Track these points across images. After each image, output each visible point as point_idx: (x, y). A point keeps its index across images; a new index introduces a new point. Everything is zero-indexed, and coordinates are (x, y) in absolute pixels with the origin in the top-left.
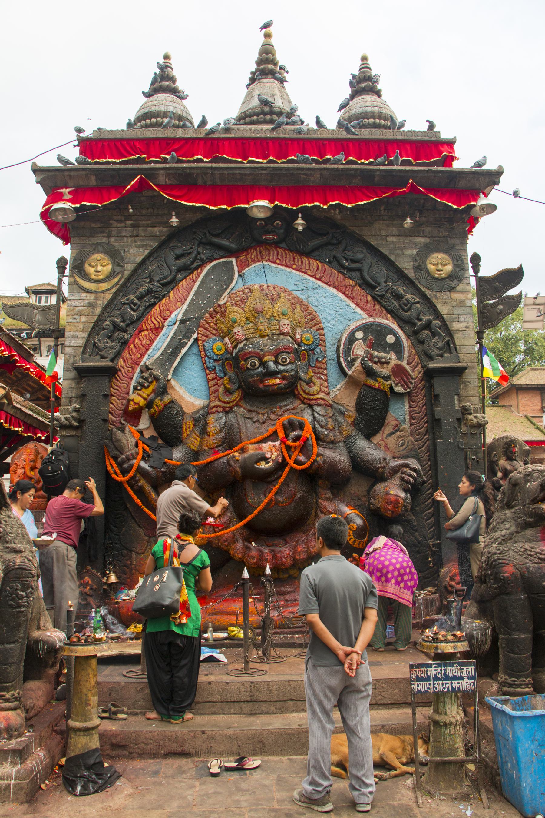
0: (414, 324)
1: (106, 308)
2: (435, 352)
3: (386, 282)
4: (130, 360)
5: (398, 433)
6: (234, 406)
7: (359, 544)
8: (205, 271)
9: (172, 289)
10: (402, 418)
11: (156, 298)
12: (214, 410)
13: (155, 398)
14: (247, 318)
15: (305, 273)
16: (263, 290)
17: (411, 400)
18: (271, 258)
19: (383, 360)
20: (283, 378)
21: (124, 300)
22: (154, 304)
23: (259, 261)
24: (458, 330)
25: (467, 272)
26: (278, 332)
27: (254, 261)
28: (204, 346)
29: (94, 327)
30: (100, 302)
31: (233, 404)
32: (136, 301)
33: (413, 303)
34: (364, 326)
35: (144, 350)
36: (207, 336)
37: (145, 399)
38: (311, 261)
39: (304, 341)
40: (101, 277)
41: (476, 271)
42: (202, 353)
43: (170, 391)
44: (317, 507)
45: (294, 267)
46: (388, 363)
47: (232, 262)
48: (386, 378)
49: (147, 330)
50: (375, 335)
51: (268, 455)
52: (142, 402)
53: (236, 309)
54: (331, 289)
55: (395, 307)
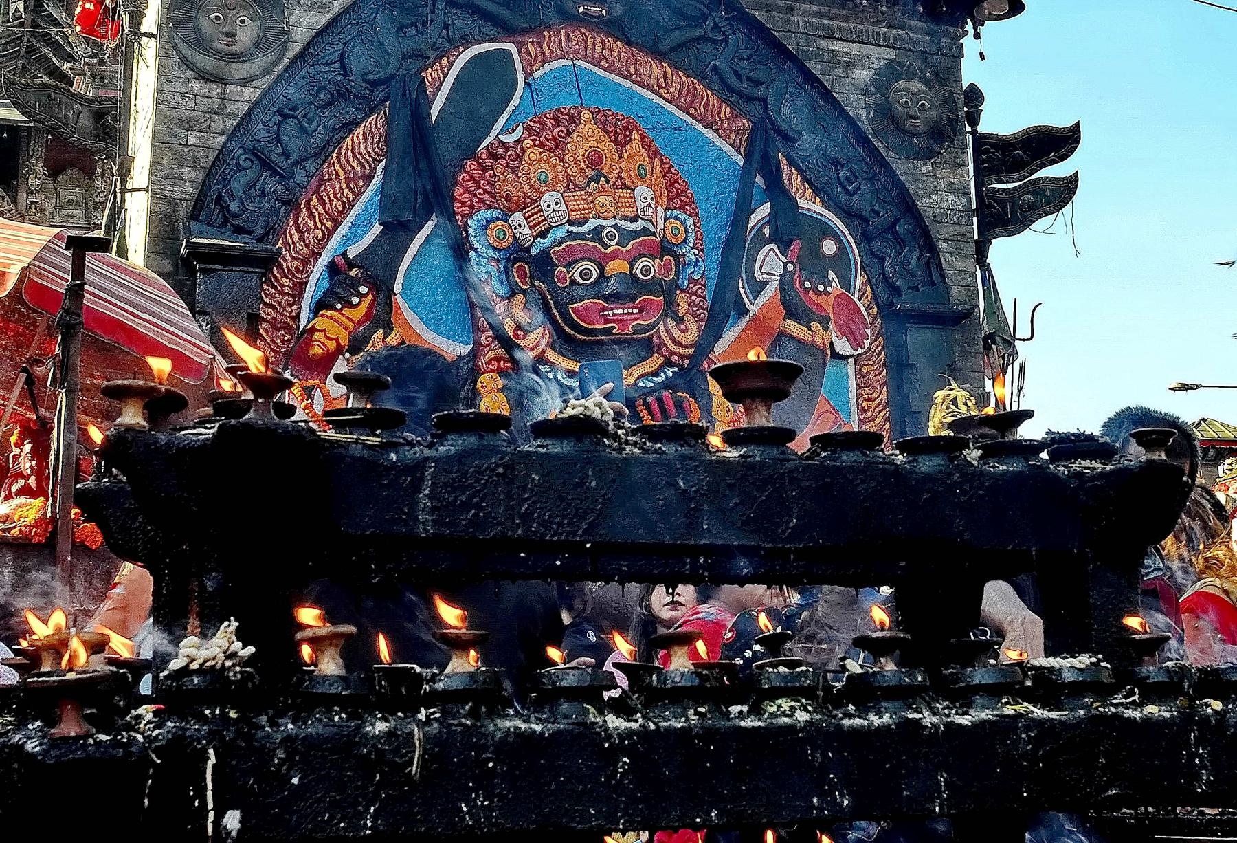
19: (821, 288)
26: (629, 212)
36: (472, 207)
54: (709, 133)
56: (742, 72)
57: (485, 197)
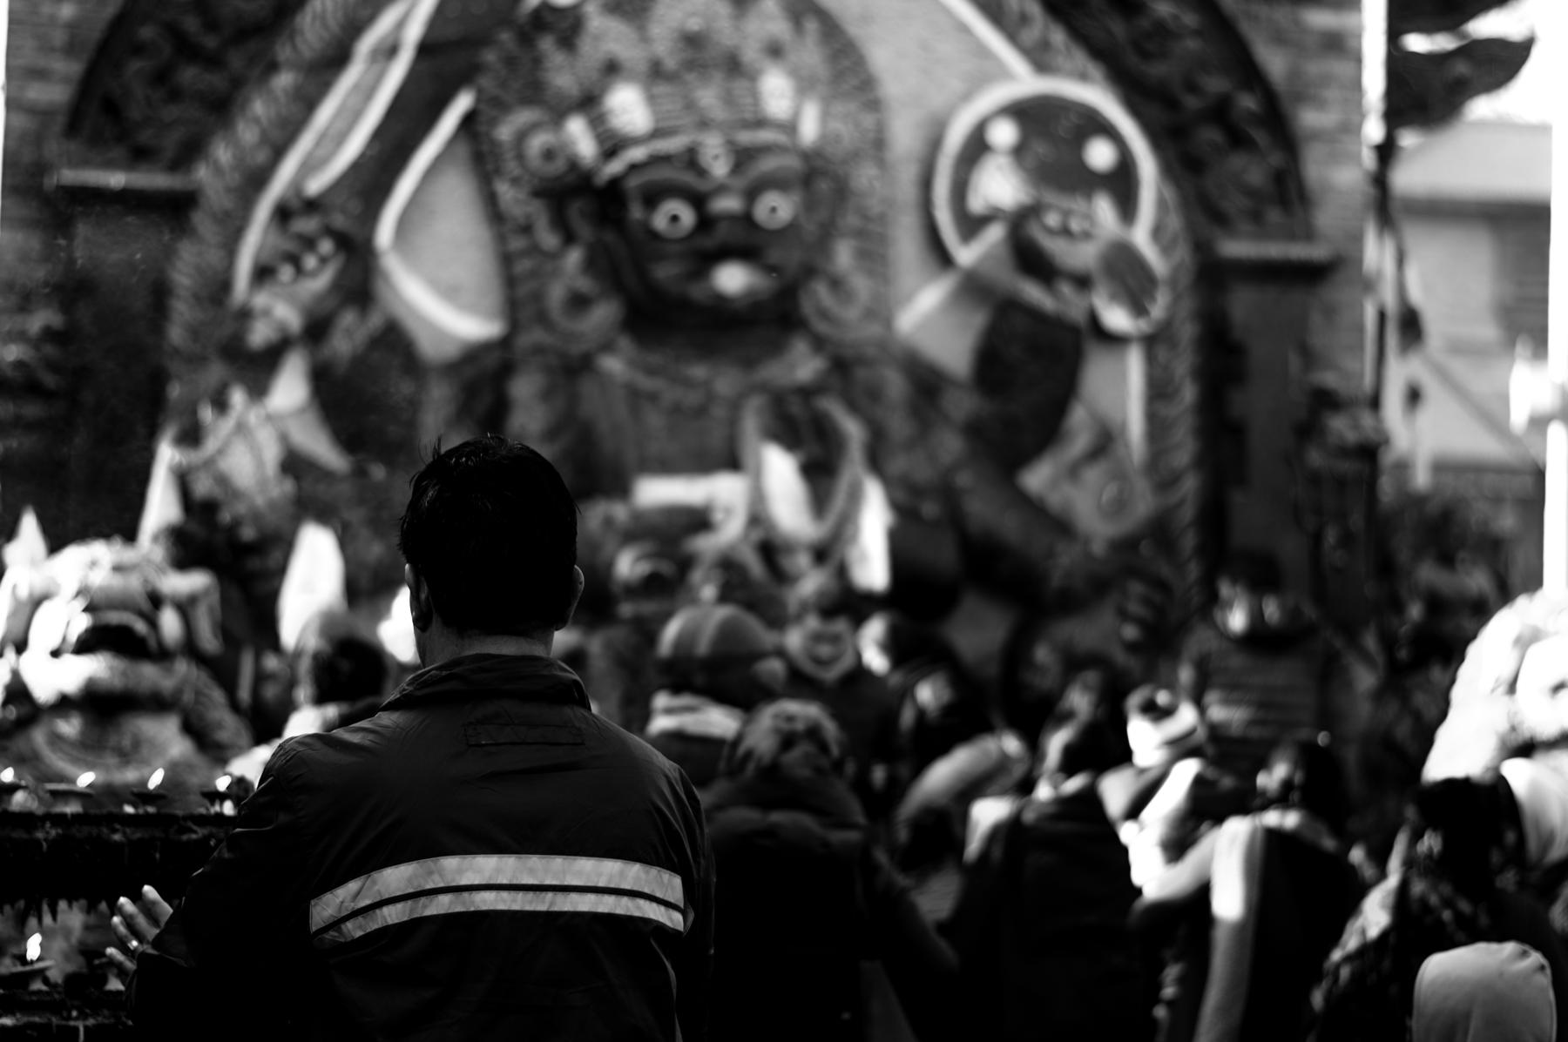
2: (1234, 203)
48: (1083, 282)
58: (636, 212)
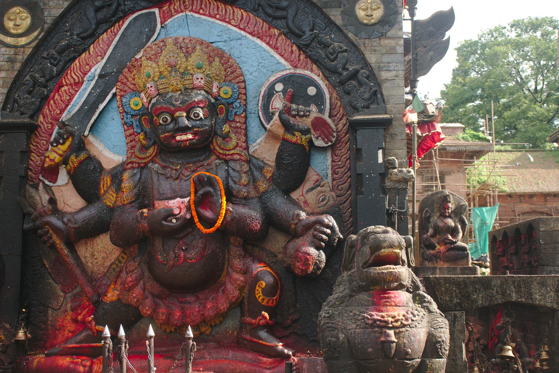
0: (340, 74)
1: (27, 63)
3: (312, 30)
4: (49, 117)
5: (319, 188)
6: (149, 162)
7: (268, 302)
8: (127, 23)
9: (93, 43)
10: (324, 172)
11: (76, 52)
12: (129, 166)
13: (71, 154)
14: (160, 72)
15: (229, 23)
16: (178, 43)
17: (333, 154)
18: (194, 7)
19: (302, 113)
20: (195, 134)
21: (45, 55)
22: (73, 60)
23: (182, 11)
24: (387, 80)
25: (400, 16)
27: (177, 12)
28: (122, 101)
29: (14, 83)
30: (20, 57)
31: (148, 159)
32: (56, 55)
33: (339, 52)
34: (284, 78)
35: (64, 106)
36: (125, 91)
37: (60, 155)
38: (236, 10)
39: (222, 95)
40: (20, 31)
41: (412, 14)
42: (121, 108)
43: (88, 147)
44: (229, 264)
45: (218, 16)
46: (307, 116)
47: (154, 13)
48: (306, 132)
49: (67, 85)
50: (295, 88)
51: (177, 211)
52: (58, 159)
53: (150, 63)
55: (321, 56)
56: (272, 4)
57: (132, 86)
58: (155, 118)
